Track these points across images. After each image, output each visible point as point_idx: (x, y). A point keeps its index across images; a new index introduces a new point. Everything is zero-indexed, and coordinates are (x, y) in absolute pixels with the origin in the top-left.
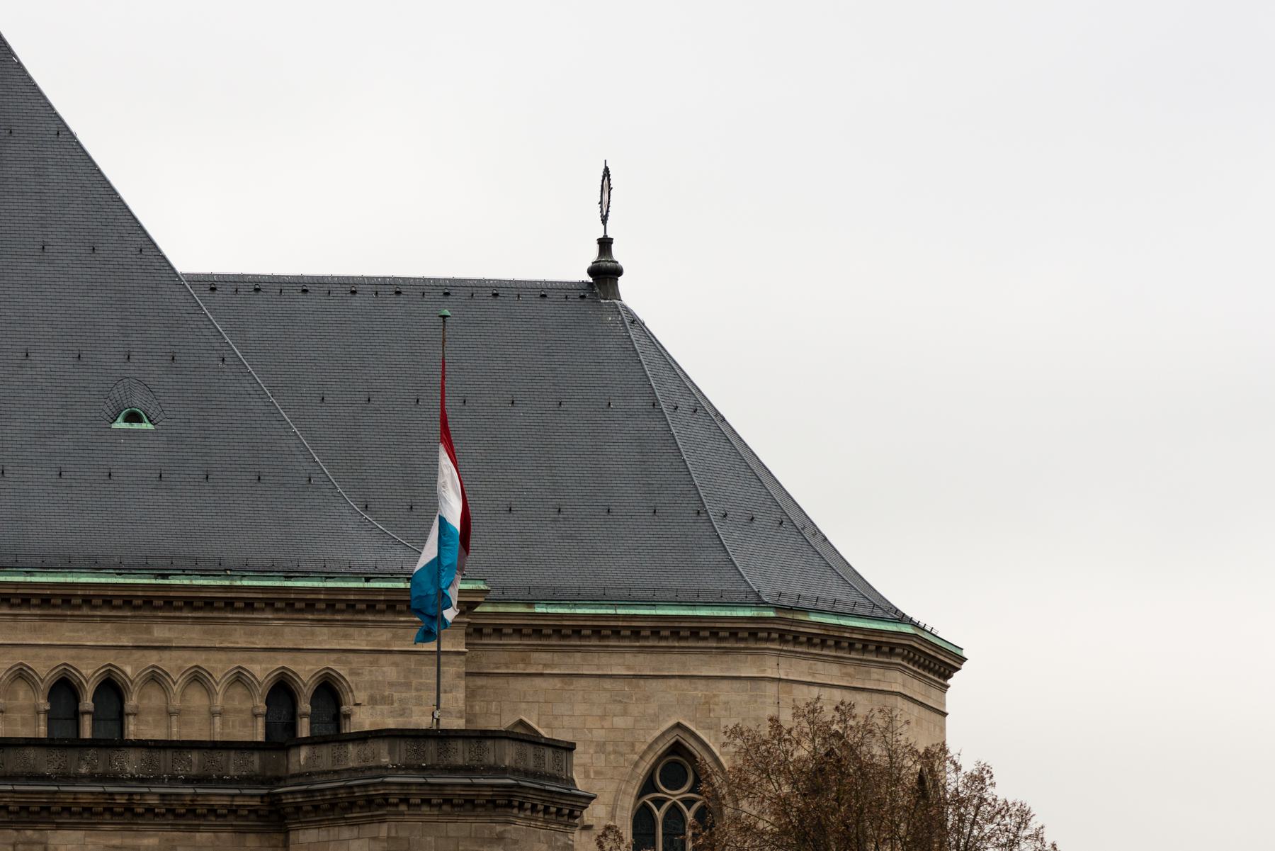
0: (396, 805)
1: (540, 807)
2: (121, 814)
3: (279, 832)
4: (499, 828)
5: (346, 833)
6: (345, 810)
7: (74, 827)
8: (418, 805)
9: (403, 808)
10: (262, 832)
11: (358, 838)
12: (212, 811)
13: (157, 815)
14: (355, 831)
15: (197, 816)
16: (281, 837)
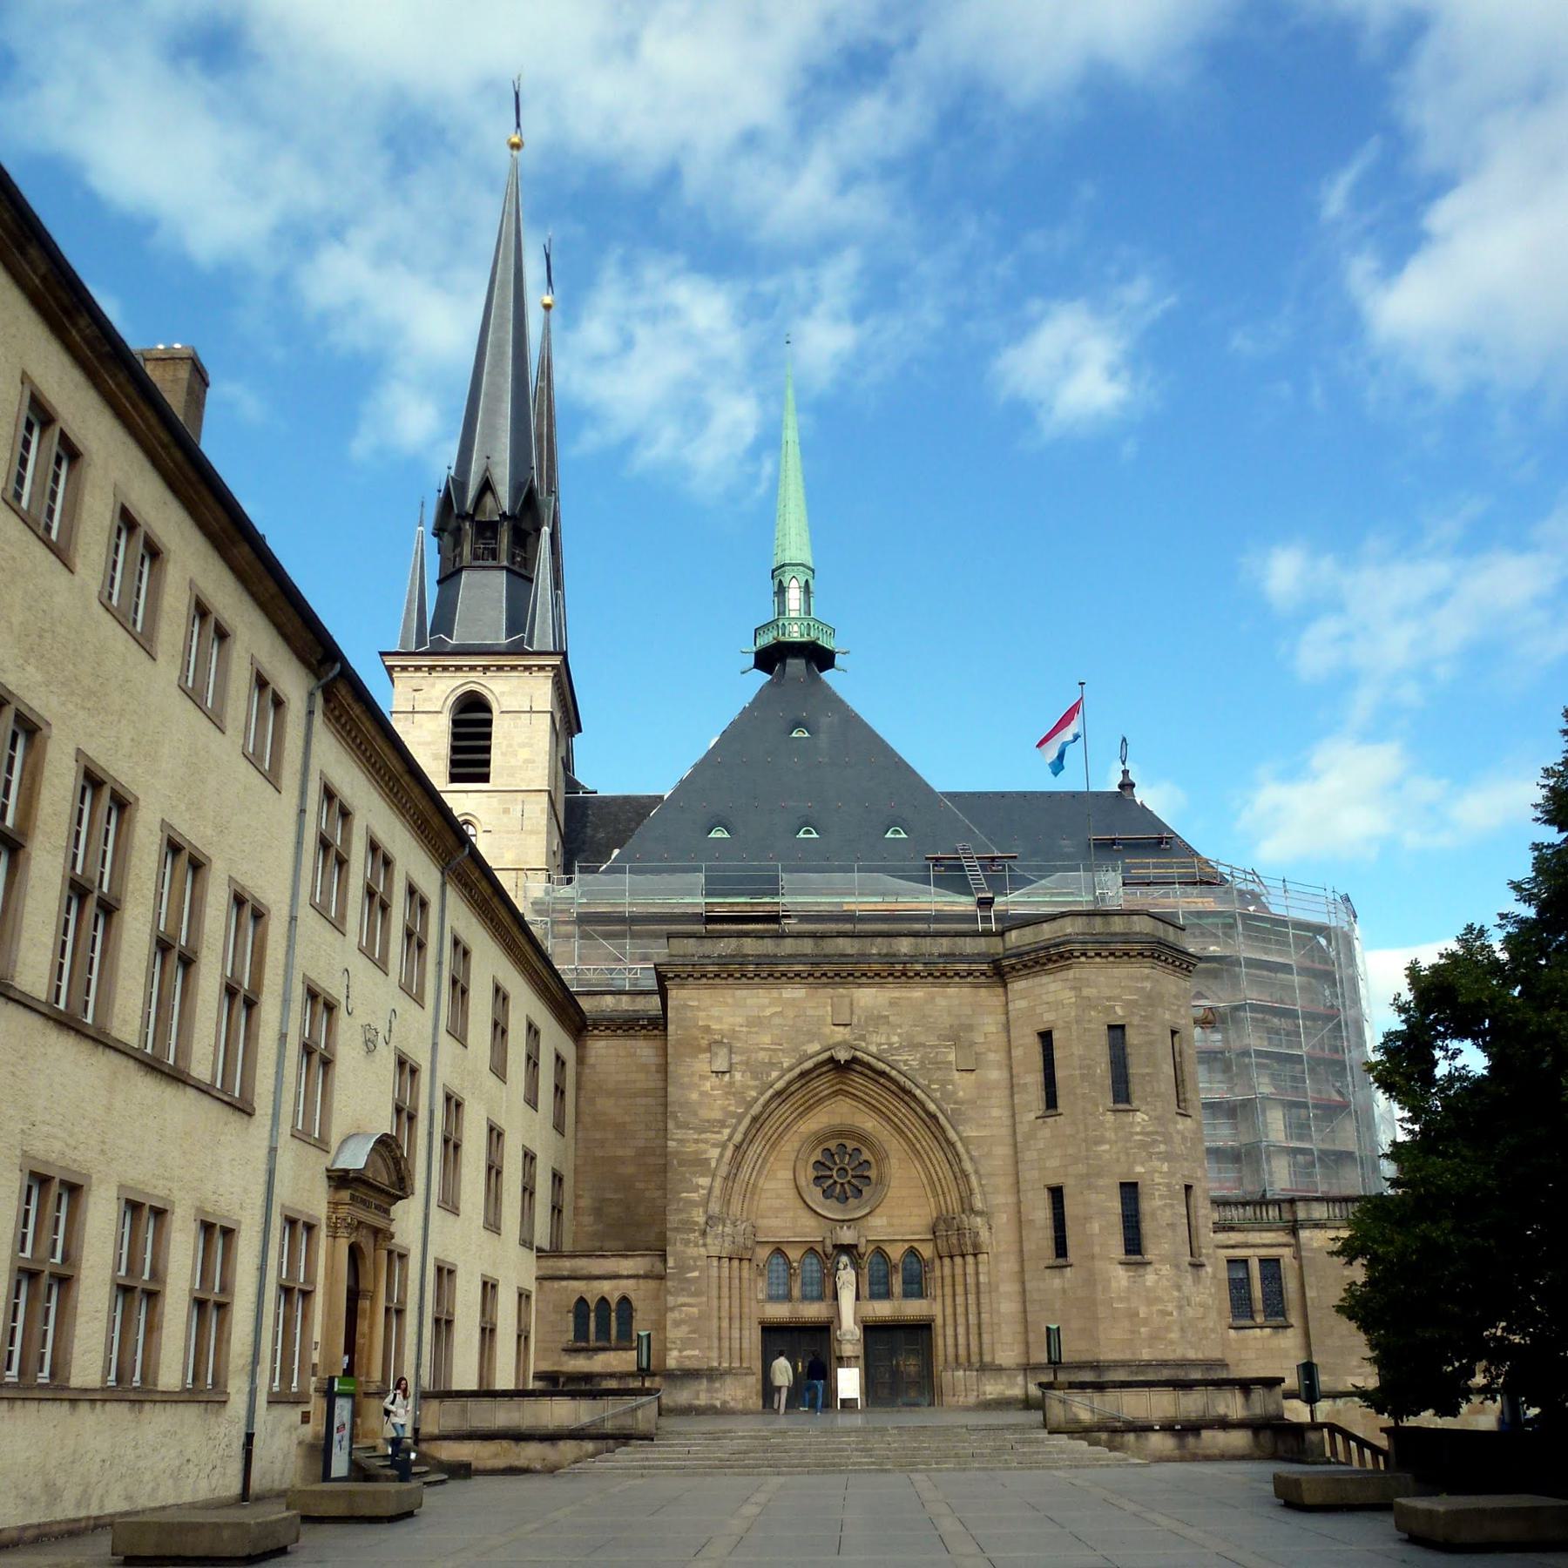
0: (1078, 957)
4: (1147, 971)
5: (1045, 979)
7: (869, 985)
9: (1083, 959)
14: (1052, 976)
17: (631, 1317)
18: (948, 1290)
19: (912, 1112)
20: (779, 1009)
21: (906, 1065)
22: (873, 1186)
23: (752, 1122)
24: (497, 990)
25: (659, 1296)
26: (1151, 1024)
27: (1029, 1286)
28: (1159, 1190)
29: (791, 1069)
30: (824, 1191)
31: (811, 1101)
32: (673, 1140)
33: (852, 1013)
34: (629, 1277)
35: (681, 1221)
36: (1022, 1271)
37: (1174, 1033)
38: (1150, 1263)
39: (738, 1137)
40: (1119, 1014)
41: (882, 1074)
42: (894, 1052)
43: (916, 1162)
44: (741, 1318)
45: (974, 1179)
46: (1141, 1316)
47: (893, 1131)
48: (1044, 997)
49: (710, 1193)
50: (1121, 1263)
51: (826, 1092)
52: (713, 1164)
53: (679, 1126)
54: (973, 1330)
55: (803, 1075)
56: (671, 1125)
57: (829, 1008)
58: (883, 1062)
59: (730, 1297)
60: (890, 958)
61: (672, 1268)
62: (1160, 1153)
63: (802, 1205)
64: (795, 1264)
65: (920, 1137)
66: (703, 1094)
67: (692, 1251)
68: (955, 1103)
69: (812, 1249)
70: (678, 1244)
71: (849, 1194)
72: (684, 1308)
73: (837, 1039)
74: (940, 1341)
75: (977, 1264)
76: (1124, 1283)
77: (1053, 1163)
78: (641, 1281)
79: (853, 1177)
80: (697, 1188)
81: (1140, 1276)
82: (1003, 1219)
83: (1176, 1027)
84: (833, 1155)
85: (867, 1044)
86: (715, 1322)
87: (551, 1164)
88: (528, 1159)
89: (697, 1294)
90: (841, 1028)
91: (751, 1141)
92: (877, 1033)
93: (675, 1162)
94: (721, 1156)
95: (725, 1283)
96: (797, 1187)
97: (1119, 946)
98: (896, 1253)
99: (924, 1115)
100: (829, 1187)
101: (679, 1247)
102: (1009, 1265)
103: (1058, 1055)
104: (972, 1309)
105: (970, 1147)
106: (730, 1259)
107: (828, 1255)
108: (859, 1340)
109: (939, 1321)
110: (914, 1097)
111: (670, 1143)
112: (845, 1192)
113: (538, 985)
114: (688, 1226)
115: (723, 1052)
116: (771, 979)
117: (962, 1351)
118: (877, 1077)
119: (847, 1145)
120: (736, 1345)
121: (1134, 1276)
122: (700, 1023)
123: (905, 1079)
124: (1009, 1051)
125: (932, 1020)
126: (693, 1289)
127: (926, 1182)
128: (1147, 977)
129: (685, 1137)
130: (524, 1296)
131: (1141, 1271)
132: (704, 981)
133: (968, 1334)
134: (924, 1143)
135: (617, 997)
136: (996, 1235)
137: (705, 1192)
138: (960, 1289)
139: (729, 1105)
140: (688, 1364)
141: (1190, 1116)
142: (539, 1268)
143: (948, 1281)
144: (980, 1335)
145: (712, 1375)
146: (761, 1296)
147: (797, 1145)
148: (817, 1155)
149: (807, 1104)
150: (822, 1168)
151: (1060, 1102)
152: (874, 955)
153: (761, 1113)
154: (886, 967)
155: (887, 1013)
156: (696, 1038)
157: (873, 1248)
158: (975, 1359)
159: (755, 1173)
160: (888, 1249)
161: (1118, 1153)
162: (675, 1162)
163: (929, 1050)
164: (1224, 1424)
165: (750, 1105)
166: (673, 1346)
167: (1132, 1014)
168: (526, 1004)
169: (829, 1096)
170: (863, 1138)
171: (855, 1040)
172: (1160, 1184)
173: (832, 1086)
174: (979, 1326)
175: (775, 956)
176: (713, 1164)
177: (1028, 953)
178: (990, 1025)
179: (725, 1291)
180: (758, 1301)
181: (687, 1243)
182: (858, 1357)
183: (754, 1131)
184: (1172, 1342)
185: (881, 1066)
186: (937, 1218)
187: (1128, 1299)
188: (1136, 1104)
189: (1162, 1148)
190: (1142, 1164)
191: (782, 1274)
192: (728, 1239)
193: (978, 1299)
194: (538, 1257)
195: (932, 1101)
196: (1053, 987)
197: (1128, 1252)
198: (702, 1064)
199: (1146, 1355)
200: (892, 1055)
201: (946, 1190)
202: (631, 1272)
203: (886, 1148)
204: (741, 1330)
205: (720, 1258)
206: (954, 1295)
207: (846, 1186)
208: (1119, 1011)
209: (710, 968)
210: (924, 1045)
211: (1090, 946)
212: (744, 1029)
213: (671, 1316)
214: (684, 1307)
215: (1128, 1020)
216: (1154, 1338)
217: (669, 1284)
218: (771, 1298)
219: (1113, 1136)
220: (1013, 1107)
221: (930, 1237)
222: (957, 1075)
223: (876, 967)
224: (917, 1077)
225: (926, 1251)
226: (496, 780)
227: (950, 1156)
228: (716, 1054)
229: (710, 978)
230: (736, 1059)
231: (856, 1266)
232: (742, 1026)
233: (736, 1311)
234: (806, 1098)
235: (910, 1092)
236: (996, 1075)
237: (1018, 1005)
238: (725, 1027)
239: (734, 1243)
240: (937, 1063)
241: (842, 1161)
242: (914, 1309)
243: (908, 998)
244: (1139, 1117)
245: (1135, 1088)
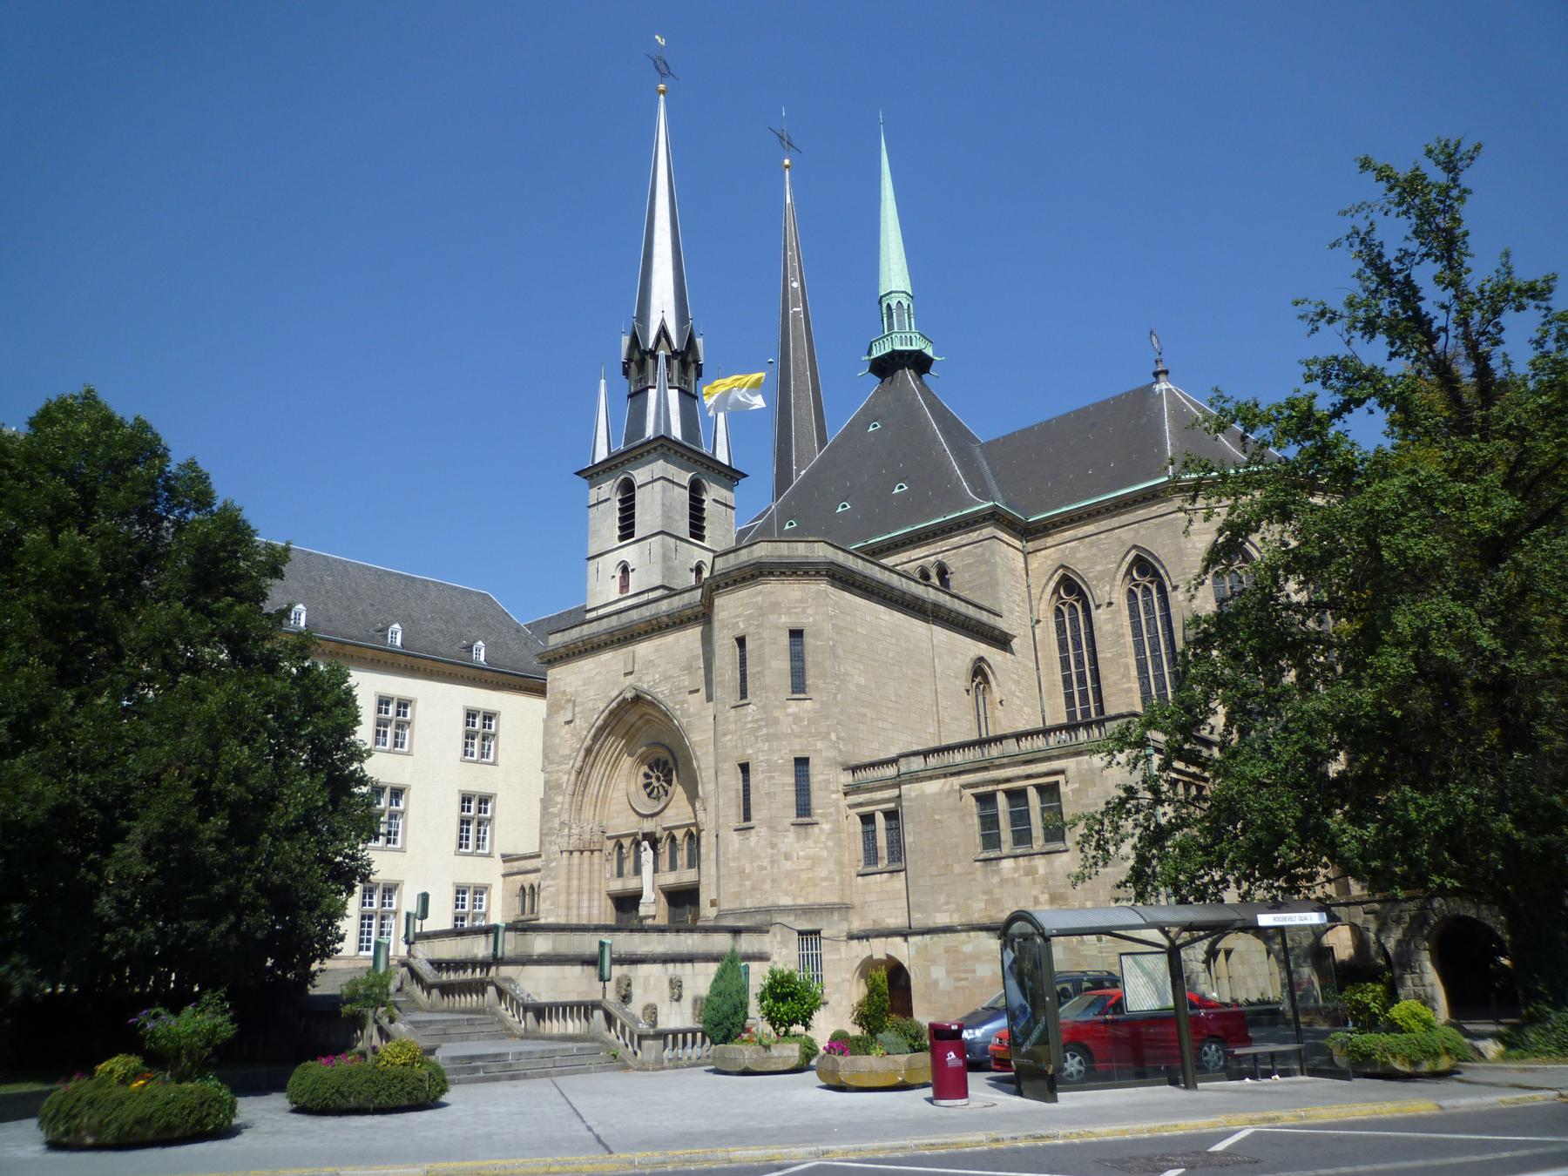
26: (761, 631)
29: (603, 711)
38: (753, 828)
40: (742, 628)
50: (735, 830)
66: (562, 738)
76: (737, 846)
89: (554, 879)
94: (568, 780)
106: (582, 852)
128: (760, 592)
146: (608, 875)
159: (602, 788)
160: (676, 833)
165: (583, 742)
167: (750, 625)
180: (606, 879)
187: (739, 858)
189: (764, 731)
199: (749, 903)
204: (590, 900)
210: (671, 677)
216: (754, 888)
226: (637, 536)
230: (577, 710)
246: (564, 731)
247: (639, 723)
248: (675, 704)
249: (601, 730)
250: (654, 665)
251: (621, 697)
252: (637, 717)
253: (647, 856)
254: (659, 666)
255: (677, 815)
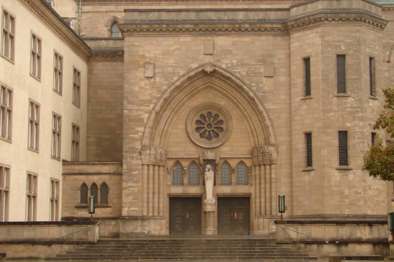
0: (324, 21)
1: (371, 23)
2: (237, 31)
3: (288, 36)
4: (358, 28)
5: (308, 32)
6: (308, 25)
8: (331, 21)
9: (326, 22)
10: (281, 36)
11: (312, 33)
12: (266, 29)
13: (249, 31)
14: (311, 31)
15: (262, 31)
16: (288, 37)
17: (107, 192)
18: (258, 182)
19: (243, 97)
20: (178, 47)
21: (239, 74)
22: (224, 132)
23: (164, 101)
24: (34, 37)
25: (120, 183)
27: (294, 179)
28: (358, 135)
29: (183, 76)
30: (201, 134)
31: (195, 92)
32: (127, 109)
33: (214, 49)
34: (106, 174)
35: (129, 148)
36: (291, 173)
37: (371, 59)
38: (351, 169)
39: (158, 108)
40: (343, 49)
41: (229, 77)
42: (234, 68)
43: (245, 122)
44: (159, 194)
45: (271, 129)
46: (346, 194)
47: (234, 106)
48: (307, 40)
49: (143, 135)
51: (202, 87)
52: (145, 121)
53: (129, 103)
54: (268, 200)
55: (189, 78)
56: (125, 102)
57: (203, 47)
58: (228, 72)
59: (153, 184)
60: (233, 22)
61: (125, 170)
62: (359, 117)
63: (190, 141)
64: (185, 169)
65: (246, 108)
66: (141, 88)
67: (135, 162)
68: (263, 92)
69: (194, 161)
70: (128, 159)
71: (213, 136)
72: (131, 188)
73: (206, 62)
74: (253, 205)
75: (271, 169)
76: (338, 178)
77: (308, 121)
78: (112, 176)
79: (215, 128)
80: (137, 132)
81: (346, 175)
82: (283, 148)
83: (372, 56)
84: (205, 117)
85: (221, 64)
86: (145, 195)
87: (71, 121)
88: (56, 118)
90: (208, 56)
91: (165, 110)
92: (226, 58)
93: (127, 120)
94: (149, 117)
95: (151, 177)
96: (187, 133)
97: (344, 15)
98: (233, 163)
99: (248, 98)
100: (203, 133)
101: (129, 160)
102: (285, 170)
103: (312, 69)
104: (268, 190)
105: (270, 114)
107: (200, 165)
108: (215, 204)
109: (253, 196)
110: (243, 89)
111: (125, 111)
112: (211, 135)
113: (61, 35)
114: (133, 150)
115: (151, 67)
116: (174, 32)
117: (263, 210)
118: (226, 80)
119: (212, 112)
120: (156, 205)
121: (343, 175)
122: (140, 54)
123: (239, 81)
124: (290, 68)
125: (253, 52)
126: (135, 179)
127: (249, 130)
129: (132, 108)
130: (54, 182)
131: (347, 173)
132: (142, 33)
133: (265, 202)
134: (248, 112)
135: (108, 41)
136: (280, 156)
137: (141, 134)
138: (263, 181)
139: (154, 93)
140: (132, 214)
141: (377, 99)
142: (64, 169)
143: (258, 177)
144: (271, 202)
145: (143, 219)
146: (169, 183)
147: (187, 113)
148: (197, 118)
149: (192, 93)
150: (200, 123)
151: (312, 92)
152: (225, 20)
153: (170, 97)
154: (231, 26)
155: (230, 49)
156: (138, 61)
157: (223, 161)
158: (268, 213)
159: (167, 125)
160: (230, 162)
161: (339, 117)
162: (127, 120)
163: (251, 67)
164: (359, 242)
165: (163, 93)
166: (125, 205)
168: (52, 43)
169: (203, 89)
170: (219, 109)
171: (215, 62)
172: (358, 132)
173: (205, 84)
174: (271, 198)
175: (177, 20)
176: (145, 121)
177: (300, 19)
178: (281, 55)
179: (151, 181)
181: (132, 158)
182: (214, 212)
183: (166, 106)
184: (360, 206)
185: (227, 74)
186: (254, 148)
188: (349, 93)
189: (360, 115)
190: (350, 122)
191: (179, 173)
192: (153, 157)
193: (271, 185)
194: (63, 164)
195: (252, 91)
196: (311, 36)
197: (341, 164)
198: (140, 73)
199: (347, 212)
200: (233, 69)
201: (258, 134)
202: (107, 172)
203: (231, 114)
204: (159, 198)
205: (148, 165)
206: (260, 184)
207: (211, 132)
208: (343, 48)
209: (144, 26)
210: (248, 65)
211: (329, 15)
212: (161, 56)
213: (124, 192)
214: (130, 188)
215: (347, 52)
216: (351, 204)
217: (124, 177)
218: (174, 184)
219: (336, 109)
220: (290, 95)
221: (250, 156)
222: (264, 79)
223: (226, 26)
224: (245, 80)
225: (248, 163)
227: (260, 118)
228: (148, 68)
229: (145, 31)
230: (157, 71)
231: (215, 170)
232: (160, 55)
233: (156, 190)
234: (192, 90)
235: (241, 87)
236: (283, 79)
237: (295, 45)
238: (152, 55)
239: (155, 158)
240: (255, 73)
241: (210, 120)
242: (241, 190)
243: (242, 41)
244: (350, 100)
245: (349, 85)
246: (143, 83)
247: (202, 87)
248: (251, 82)
249: (179, 89)
250: (232, 53)
251: (200, 69)
252: (203, 83)
253: (209, 175)
254: (237, 55)
255: (231, 150)
